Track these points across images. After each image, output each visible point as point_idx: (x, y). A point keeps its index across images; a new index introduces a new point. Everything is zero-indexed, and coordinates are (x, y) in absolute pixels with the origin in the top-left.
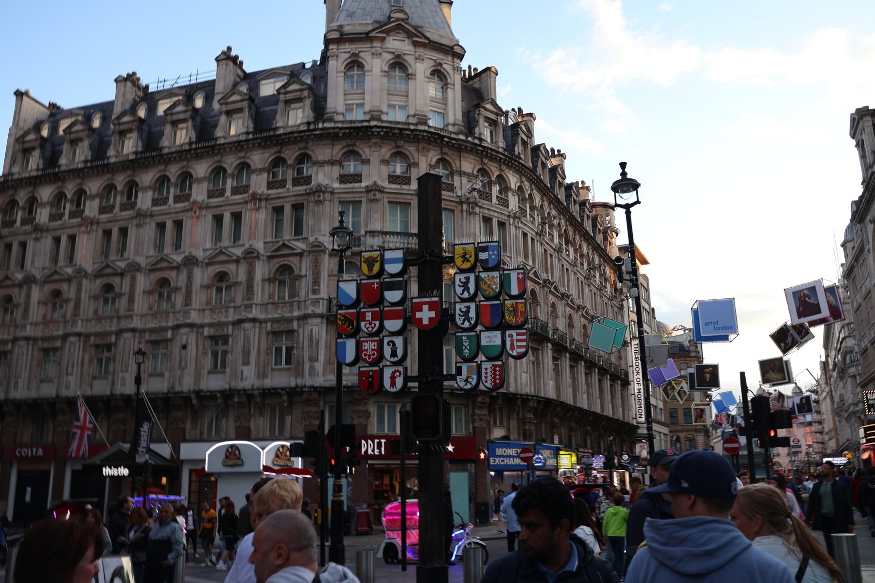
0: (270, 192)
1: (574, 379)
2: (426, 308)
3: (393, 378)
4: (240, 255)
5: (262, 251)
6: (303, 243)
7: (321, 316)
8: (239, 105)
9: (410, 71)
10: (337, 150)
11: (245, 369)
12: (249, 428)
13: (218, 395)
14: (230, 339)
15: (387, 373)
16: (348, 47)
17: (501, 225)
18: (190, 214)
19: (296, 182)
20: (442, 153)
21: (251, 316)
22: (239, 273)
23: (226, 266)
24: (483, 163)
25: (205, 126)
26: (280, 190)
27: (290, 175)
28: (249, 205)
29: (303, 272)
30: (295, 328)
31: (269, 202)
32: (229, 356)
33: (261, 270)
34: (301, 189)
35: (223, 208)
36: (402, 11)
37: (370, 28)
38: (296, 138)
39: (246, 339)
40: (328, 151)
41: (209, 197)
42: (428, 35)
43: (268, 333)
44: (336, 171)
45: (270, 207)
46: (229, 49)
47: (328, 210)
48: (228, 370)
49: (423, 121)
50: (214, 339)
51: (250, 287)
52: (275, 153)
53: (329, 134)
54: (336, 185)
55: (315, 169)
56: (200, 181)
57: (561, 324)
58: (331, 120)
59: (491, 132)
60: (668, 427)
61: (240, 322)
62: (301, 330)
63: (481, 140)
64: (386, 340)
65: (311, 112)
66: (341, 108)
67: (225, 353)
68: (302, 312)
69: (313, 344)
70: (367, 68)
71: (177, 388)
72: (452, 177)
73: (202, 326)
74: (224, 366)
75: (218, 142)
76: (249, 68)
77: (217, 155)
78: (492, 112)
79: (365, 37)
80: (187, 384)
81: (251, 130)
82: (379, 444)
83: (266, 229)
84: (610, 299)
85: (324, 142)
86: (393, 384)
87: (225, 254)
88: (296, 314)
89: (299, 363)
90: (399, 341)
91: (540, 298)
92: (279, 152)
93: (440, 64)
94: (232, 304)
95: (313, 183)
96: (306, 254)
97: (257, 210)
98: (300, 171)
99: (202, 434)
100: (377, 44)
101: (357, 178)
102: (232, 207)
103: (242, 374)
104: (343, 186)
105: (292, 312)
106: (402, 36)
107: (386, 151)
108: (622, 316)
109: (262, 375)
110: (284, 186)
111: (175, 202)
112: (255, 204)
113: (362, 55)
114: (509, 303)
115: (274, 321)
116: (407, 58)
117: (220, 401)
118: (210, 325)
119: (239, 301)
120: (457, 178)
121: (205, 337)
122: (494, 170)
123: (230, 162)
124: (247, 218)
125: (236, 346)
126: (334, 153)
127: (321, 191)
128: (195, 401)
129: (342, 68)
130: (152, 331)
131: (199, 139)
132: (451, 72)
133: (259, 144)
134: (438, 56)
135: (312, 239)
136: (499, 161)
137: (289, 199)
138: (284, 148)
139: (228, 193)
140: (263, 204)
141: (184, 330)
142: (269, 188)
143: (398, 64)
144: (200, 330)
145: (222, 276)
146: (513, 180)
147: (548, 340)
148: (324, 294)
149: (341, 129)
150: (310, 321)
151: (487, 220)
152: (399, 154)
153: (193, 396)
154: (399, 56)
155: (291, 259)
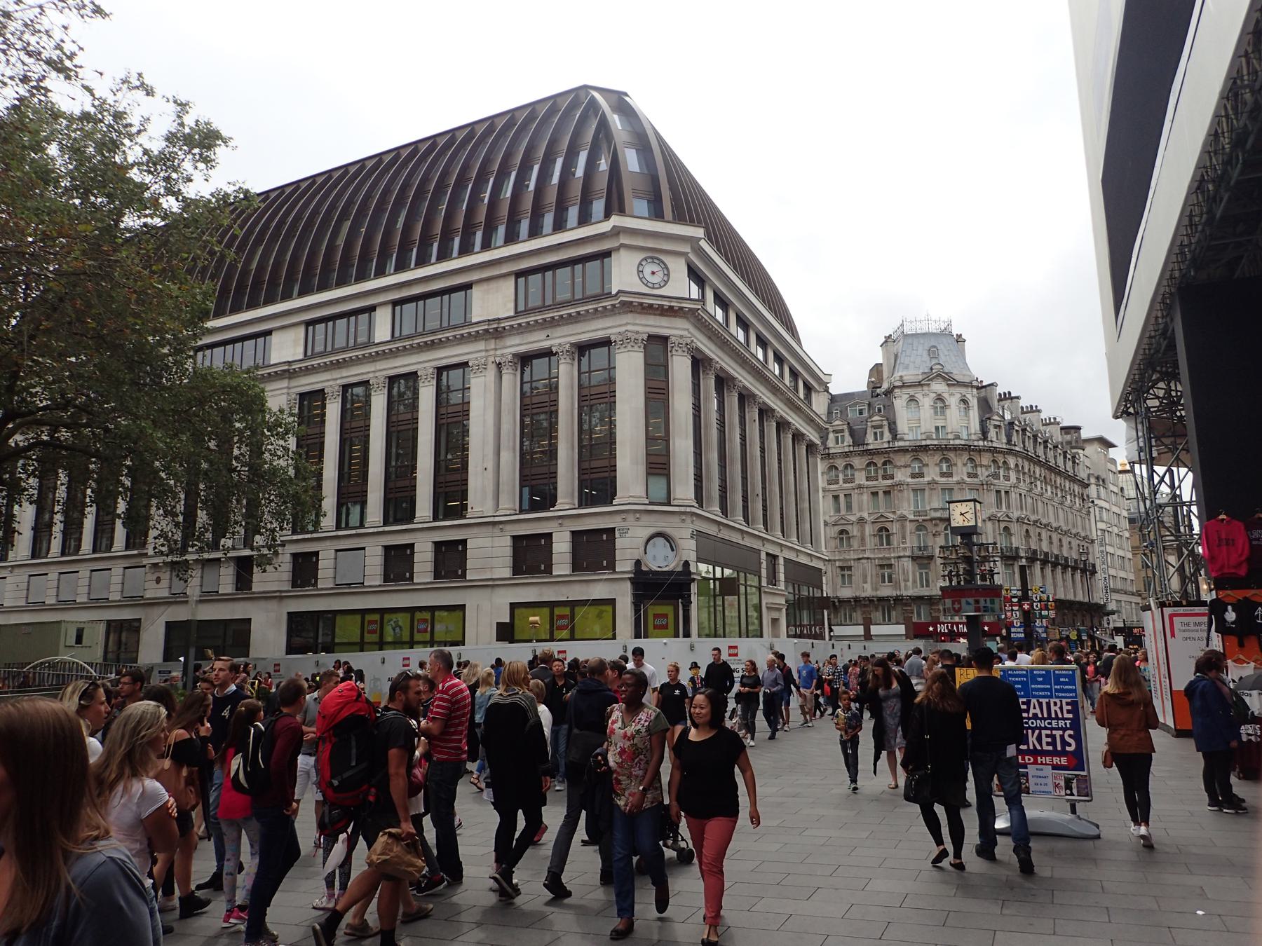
1: (1054, 578)
16: (905, 391)
17: (1007, 492)
19: (884, 478)
22: (854, 531)
27: (881, 473)
33: (869, 529)
34: (889, 482)
37: (920, 378)
39: (864, 569)
44: (909, 471)
49: (957, 437)
50: (842, 568)
51: (863, 539)
54: (909, 480)
57: (1045, 548)
58: (902, 439)
66: (906, 431)
67: (850, 576)
74: (850, 582)
79: (919, 384)
91: (1031, 534)
98: (885, 470)
101: (921, 475)
106: (940, 380)
107: (938, 458)
115: (880, 559)
119: (856, 547)
122: (1001, 459)
123: (840, 463)
124: (855, 498)
135: (898, 513)
136: (1004, 453)
143: (940, 398)
145: (842, 532)
146: (1012, 462)
151: (998, 492)
152: (947, 460)
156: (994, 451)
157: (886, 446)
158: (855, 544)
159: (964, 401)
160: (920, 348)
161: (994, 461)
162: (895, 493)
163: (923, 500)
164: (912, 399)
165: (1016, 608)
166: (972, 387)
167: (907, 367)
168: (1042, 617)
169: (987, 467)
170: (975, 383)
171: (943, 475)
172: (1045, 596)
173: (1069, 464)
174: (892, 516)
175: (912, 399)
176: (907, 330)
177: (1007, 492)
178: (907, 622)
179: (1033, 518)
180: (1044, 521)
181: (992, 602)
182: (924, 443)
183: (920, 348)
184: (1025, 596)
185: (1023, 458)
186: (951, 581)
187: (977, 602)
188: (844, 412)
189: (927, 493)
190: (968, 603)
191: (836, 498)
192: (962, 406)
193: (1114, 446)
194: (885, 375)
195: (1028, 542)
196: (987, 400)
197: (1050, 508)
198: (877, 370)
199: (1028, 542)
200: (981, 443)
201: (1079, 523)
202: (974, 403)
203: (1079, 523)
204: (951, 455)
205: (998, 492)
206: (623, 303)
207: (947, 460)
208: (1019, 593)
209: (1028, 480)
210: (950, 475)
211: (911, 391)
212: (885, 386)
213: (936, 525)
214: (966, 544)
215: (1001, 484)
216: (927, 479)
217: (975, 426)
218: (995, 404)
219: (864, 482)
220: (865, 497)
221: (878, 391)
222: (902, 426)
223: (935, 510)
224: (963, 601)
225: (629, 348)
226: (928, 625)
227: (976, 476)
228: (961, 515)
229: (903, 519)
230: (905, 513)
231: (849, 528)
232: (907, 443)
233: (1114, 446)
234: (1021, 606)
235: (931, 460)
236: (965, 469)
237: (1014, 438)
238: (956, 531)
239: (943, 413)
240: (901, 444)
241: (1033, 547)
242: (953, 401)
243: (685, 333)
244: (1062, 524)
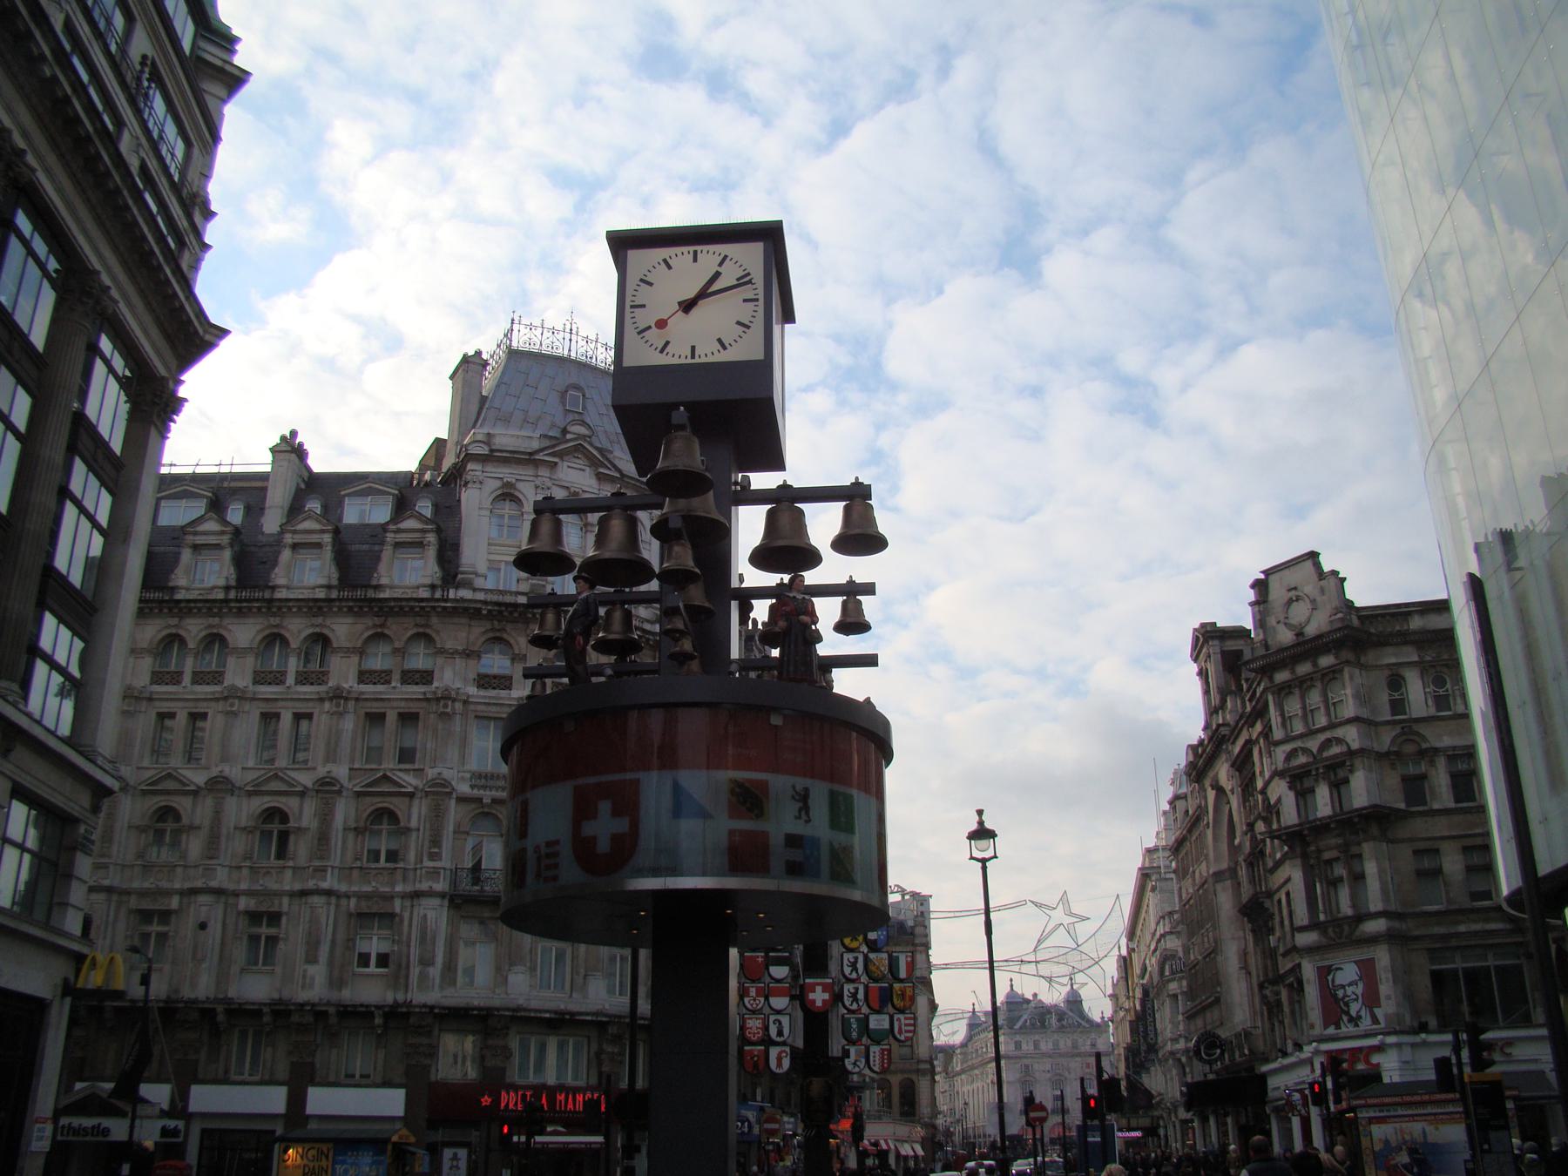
0: (363, 688)
2: (819, 989)
3: (779, 1059)
4: (310, 785)
5: (345, 782)
6: (415, 777)
7: (442, 895)
8: (314, 538)
10: (476, 633)
11: (312, 970)
12: (312, 1064)
13: (266, 1010)
14: (284, 920)
15: (774, 1052)
18: (221, 706)
21: (325, 885)
22: (306, 814)
23: (283, 799)
25: (252, 561)
26: (380, 688)
28: (327, 705)
29: (414, 823)
30: (398, 910)
31: (360, 704)
32: (281, 945)
33: (343, 812)
34: (416, 690)
35: (281, 704)
36: (584, 423)
37: (535, 445)
38: (412, 608)
41: (256, 682)
43: (350, 915)
44: (473, 668)
45: (363, 712)
46: (294, 434)
47: (458, 729)
48: (278, 970)
50: (254, 917)
51: (323, 838)
52: (375, 626)
53: (466, 609)
54: (472, 690)
55: (440, 660)
56: (242, 652)
58: (468, 584)
61: (304, 893)
62: (406, 915)
64: (772, 1018)
65: (436, 568)
66: (482, 568)
67: (272, 941)
68: (409, 888)
69: (426, 938)
71: (187, 993)
73: (236, 894)
75: (278, 595)
76: (319, 463)
77: (274, 615)
79: (528, 459)
80: (202, 987)
81: (335, 582)
82: (524, 1096)
83: (353, 749)
85: (456, 620)
86: (779, 1064)
87: (282, 779)
88: (399, 888)
89: (400, 966)
90: (785, 1020)
92: (382, 626)
94: (291, 863)
95: (436, 684)
96: (419, 795)
97: (341, 714)
99: (226, 1072)
100: (544, 472)
102: (297, 704)
103: (304, 977)
104: (482, 693)
105: (393, 885)
106: (581, 462)
109: (336, 982)
110: (389, 682)
111: (195, 682)
112: (338, 705)
113: (520, 486)
114: (897, 986)
115: (361, 896)
117: (266, 1019)
118: (250, 893)
121: (239, 913)
123: (297, 629)
125: (293, 935)
126: (472, 638)
127: (449, 698)
128: (221, 1018)
129: (487, 503)
130: (143, 894)
131: (242, 583)
133: (350, 609)
135: (431, 773)
137: (395, 704)
138: (390, 620)
139: (290, 680)
140: (351, 704)
141: (203, 899)
142: (361, 681)
144: (231, 900)
145: (274, 815)
148: (446, 862)
149: (485, 602)
150: (425, 901)
153: (220, 1009)
155: (395, 800)
157: (425, 594)
158: (301, 849)
165: (779, 1002)
174: (410, 781)
178: (415, 1080)
187: (749, 800)
188: (332, 510)
191: (270, 718)
211: (507, 473)
219: (350, 683)
220: (349, 724)
230: (447, 774)
231: (290, 804)
232: (480, 596)
240: (465, 593)
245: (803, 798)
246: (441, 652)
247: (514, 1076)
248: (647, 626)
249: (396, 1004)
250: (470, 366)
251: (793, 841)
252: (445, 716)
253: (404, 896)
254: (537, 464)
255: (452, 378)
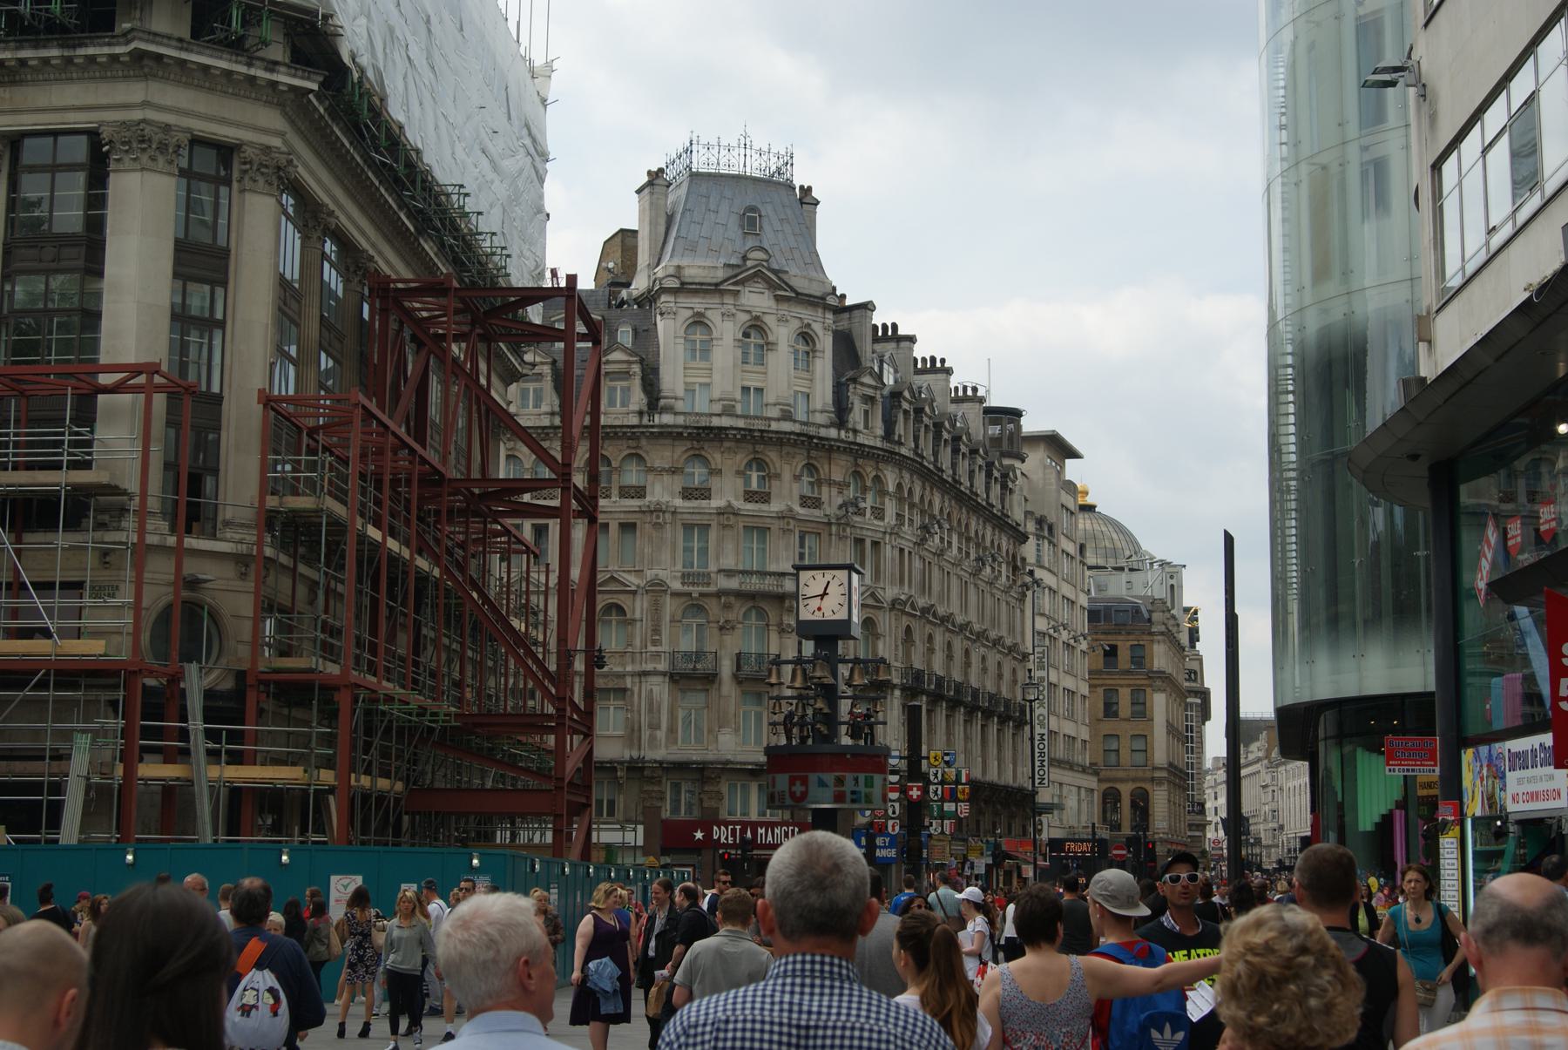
7: (664, 674)
9: (771, 339)
15: (890, 823)
17: (876, 544)
20: (809, 457)
24: (857, 465)
29: (638, 615)
36: (762, 249)
37: (720, 274)
40: (668, 454)
42: (795, 283)
44: (678, 483)
49: (787, 416)
54: (678, 502)
55: (650, 477)
57: (938, 668)
58: (668, 409)
59: (866, 412)
60: (1096, 773)
62: (636, 689)
63: (855, 431)
65: (642, 396)
66: (680, 393)
68: (637, 668)
69: (653, 708)
70: (715, 335)
72: (820, 487)
78: (870, 386)
79: (715, 289)
82: (734, 831)
84: (1006, 591)
85: (662, 441)
88: (629, 668)
90: (897, 805)
91: (916, 637)
93: (809, 325)
100: (729, 300)
101: (705, 493)
104: (688, 504)
105: (624, 665)
106: (760, 286)
107: (741, 459)
108: (1022, 611)
113: (709, 314)
116: (767, 319)
120: (825, 489)
122: (869, 471)
132: (820, 332)
134: (806, 314)
135: (650, 574)
143: (756, 326)
146: (891, 478)
147: (923, 692)
148: (665, 647)
149: (686, 427)
152: (760, 464)
154: (757, 318)
155: (622, 597)
156: (858, 452)
157: (634, 420)
159: (806, 336)
160: (725, 207)
161: (857, 475)
162: (645, 528)
163: (704, 552)
164: (699, 321)
166: (827, 307)
167: (692, 249)
168: (943, 816)
169: (842, 486)
170: (831, 301)
171: (750, 496)
172: (951, 772)
173: (996, 489)
174: (633, 580)
175: (699, 321)
176: (701, 163)
177: (876, 544)
178: (649, 817)
179: (922, 602)
180: (941, 611)
181: (869, 783)
182: (716, 422)
183: (725, 207)
184: (914, 770)
185: (912, 472)
186: (789, 738)
187: (840, 781)
189: (713, 534)
190: (822, 784)
192: (802, 347)
193: (1075, 455)
194: (643, 258)
195: (907, 655)
196: (853, 339)
197: (954, 582)
198: (624, 242)
199: (907, 655)
200: (833, 433)
201: (1004, 618)
202: (826, 343)
203: (1004, 618)
204: (772, 455)
205: (859, 541)
206: (139, 56)
207: (760, 464)
208: (903, 765)
209: (917, 520)
210: (764, 498)
211: (698, 303)
212: (640, 284)
213: (727, 607)
214: (827, 659)
215: (869, 525)
216: (716, 503)
217: (823, 393)
218: (866, 348)
221: (624, 294)
222: (672, 379)
223: (729, 573)
224: (813, 777)
225: (145, 158)
226: (694, 826)
227: (815, 503)
228: (828, 597)
229: (657, 588)
230: (663, 574)
232: (680, 420)
233: (1075, 455)
234: (904, 791)
235: (728, 461)
236: (796, 486)
237: (900, 429)
238: (807, 630)
239: (761, 361)
240: (667, 419)
241: (918, 664)
242: (783, 334)
243: (276, 142)
244: (972, 617)
245: (856, 780)
246: (651, 470)
247: (724, 815)
248: (823, 432)
249: (632, 760)
250: (656, 178)
251: (853, 793)
252: (658, 526)
253: (633, 675)
254: (722, 293)
255: (639, 192)
